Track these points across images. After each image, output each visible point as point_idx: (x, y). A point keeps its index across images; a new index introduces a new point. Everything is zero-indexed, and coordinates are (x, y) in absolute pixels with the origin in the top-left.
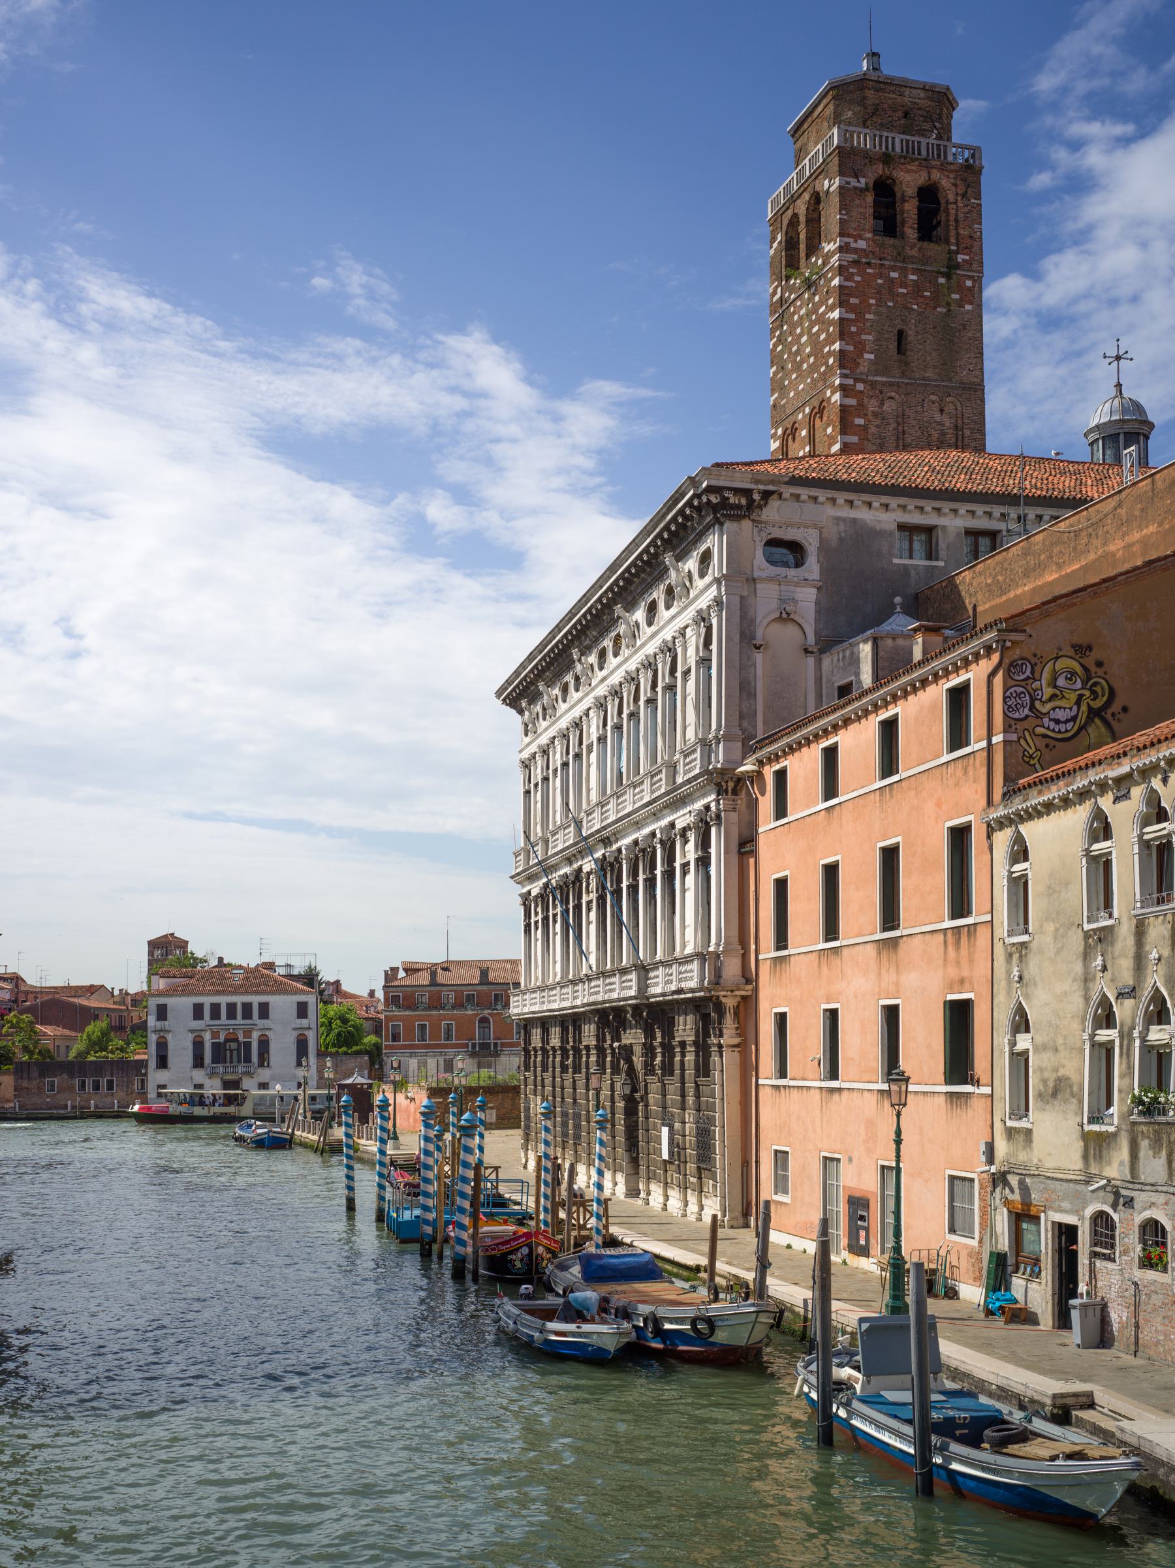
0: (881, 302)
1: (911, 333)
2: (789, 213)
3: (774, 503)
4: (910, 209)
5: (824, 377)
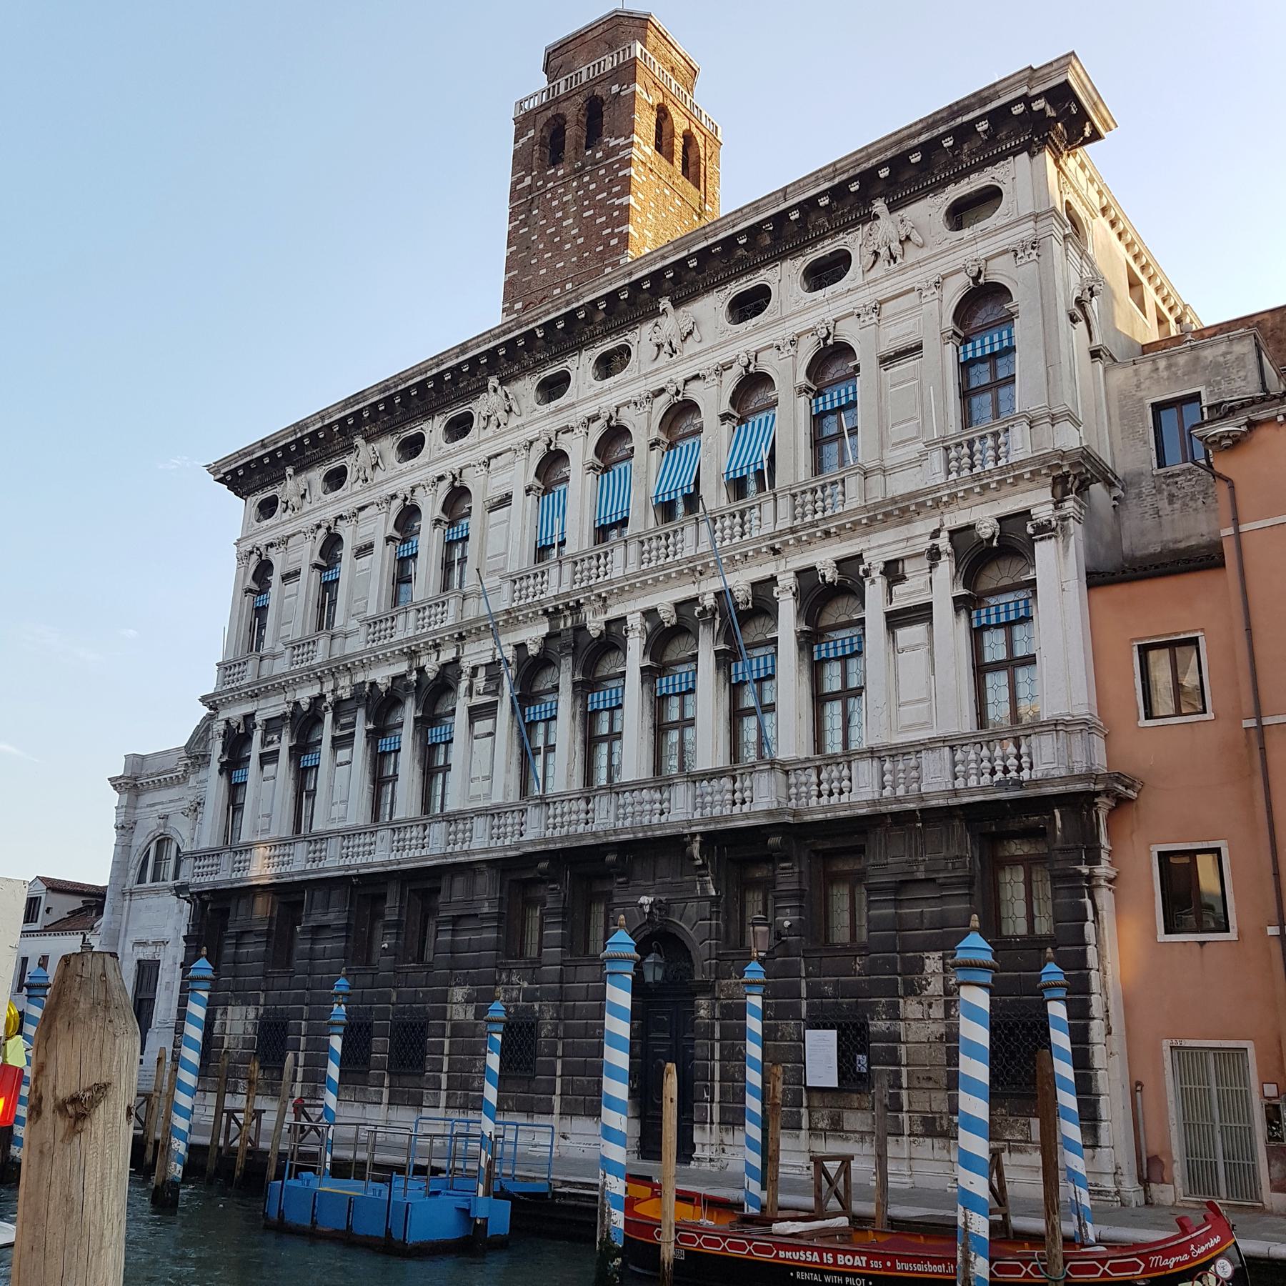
2: (550, 113)
4: (678, 143)
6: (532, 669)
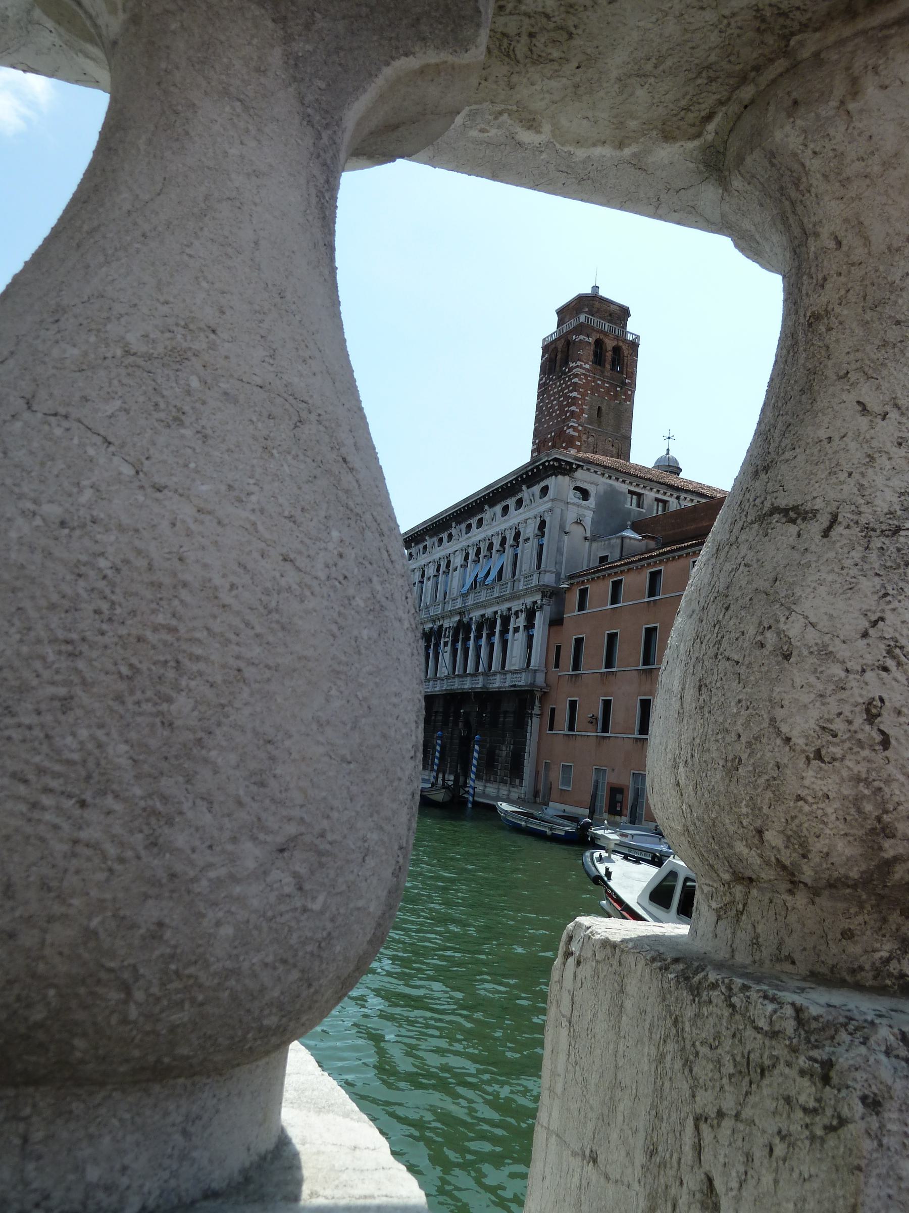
0: (592, 393)
1: (604, 408)
3: (580, 470)
4: (609, 354)
5: (564, 421)
6: (456, 630)
